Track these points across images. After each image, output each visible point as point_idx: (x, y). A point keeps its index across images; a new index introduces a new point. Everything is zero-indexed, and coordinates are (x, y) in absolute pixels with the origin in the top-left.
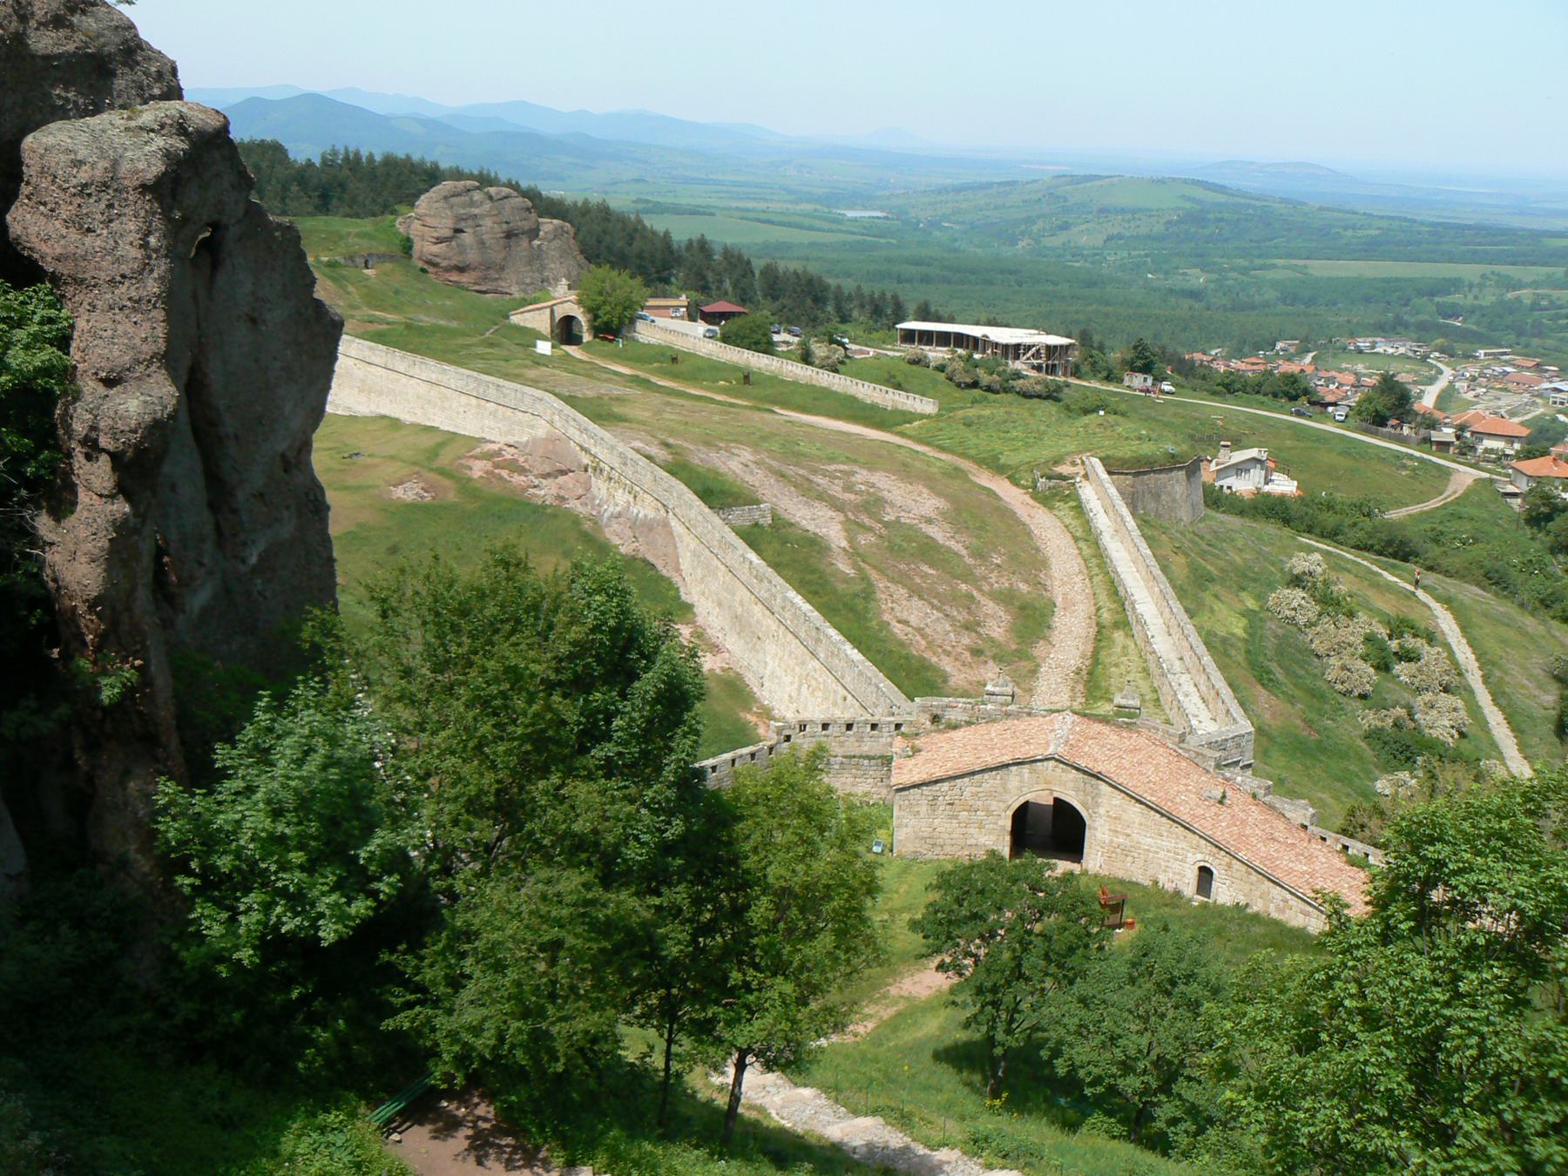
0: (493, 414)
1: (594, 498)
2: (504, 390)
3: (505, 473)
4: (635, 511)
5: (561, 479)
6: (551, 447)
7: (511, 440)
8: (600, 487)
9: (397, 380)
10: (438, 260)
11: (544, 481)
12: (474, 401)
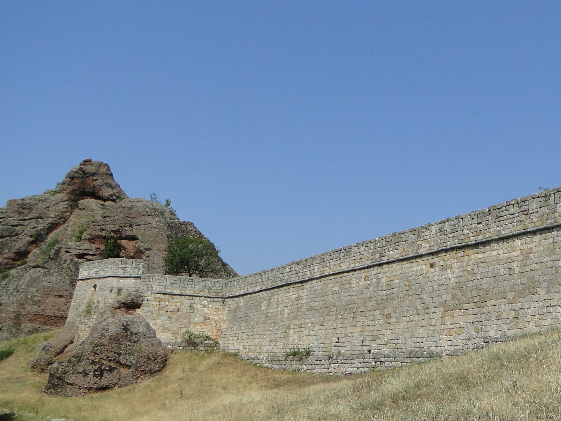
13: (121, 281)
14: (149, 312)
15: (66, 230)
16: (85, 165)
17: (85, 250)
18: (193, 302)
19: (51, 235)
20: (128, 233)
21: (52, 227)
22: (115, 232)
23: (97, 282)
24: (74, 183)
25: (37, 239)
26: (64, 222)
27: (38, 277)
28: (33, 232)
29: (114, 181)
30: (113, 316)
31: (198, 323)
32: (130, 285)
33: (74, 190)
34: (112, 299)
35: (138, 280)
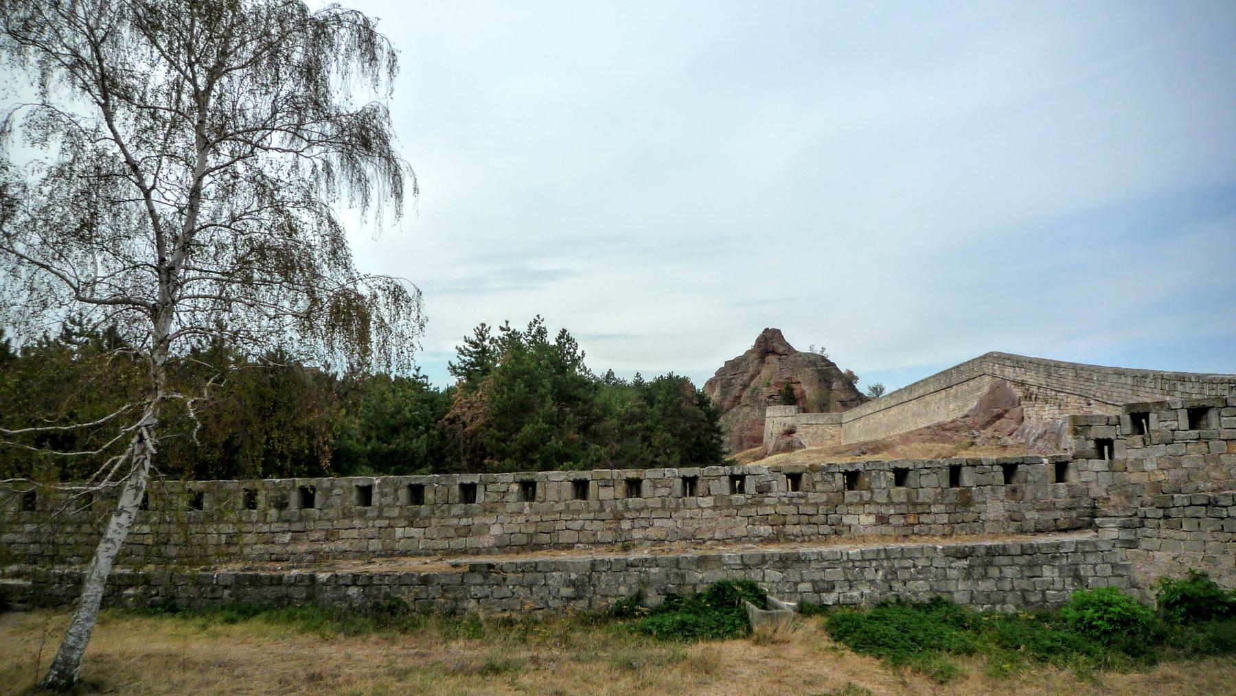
0: (956, 397)
1: (1024, 430)
3: (949, 434)
5: (997, 422)
6: (991, 397)
7: (965, 411)
8: (1030, 411)
11: (982, 431)
12: (944, 393)
19: (752, 383)
21: (753, 377)
25: (745, 386)
28: (741, 382)
32: (790, 421)
33: (762, 351)
34: (781, 429)
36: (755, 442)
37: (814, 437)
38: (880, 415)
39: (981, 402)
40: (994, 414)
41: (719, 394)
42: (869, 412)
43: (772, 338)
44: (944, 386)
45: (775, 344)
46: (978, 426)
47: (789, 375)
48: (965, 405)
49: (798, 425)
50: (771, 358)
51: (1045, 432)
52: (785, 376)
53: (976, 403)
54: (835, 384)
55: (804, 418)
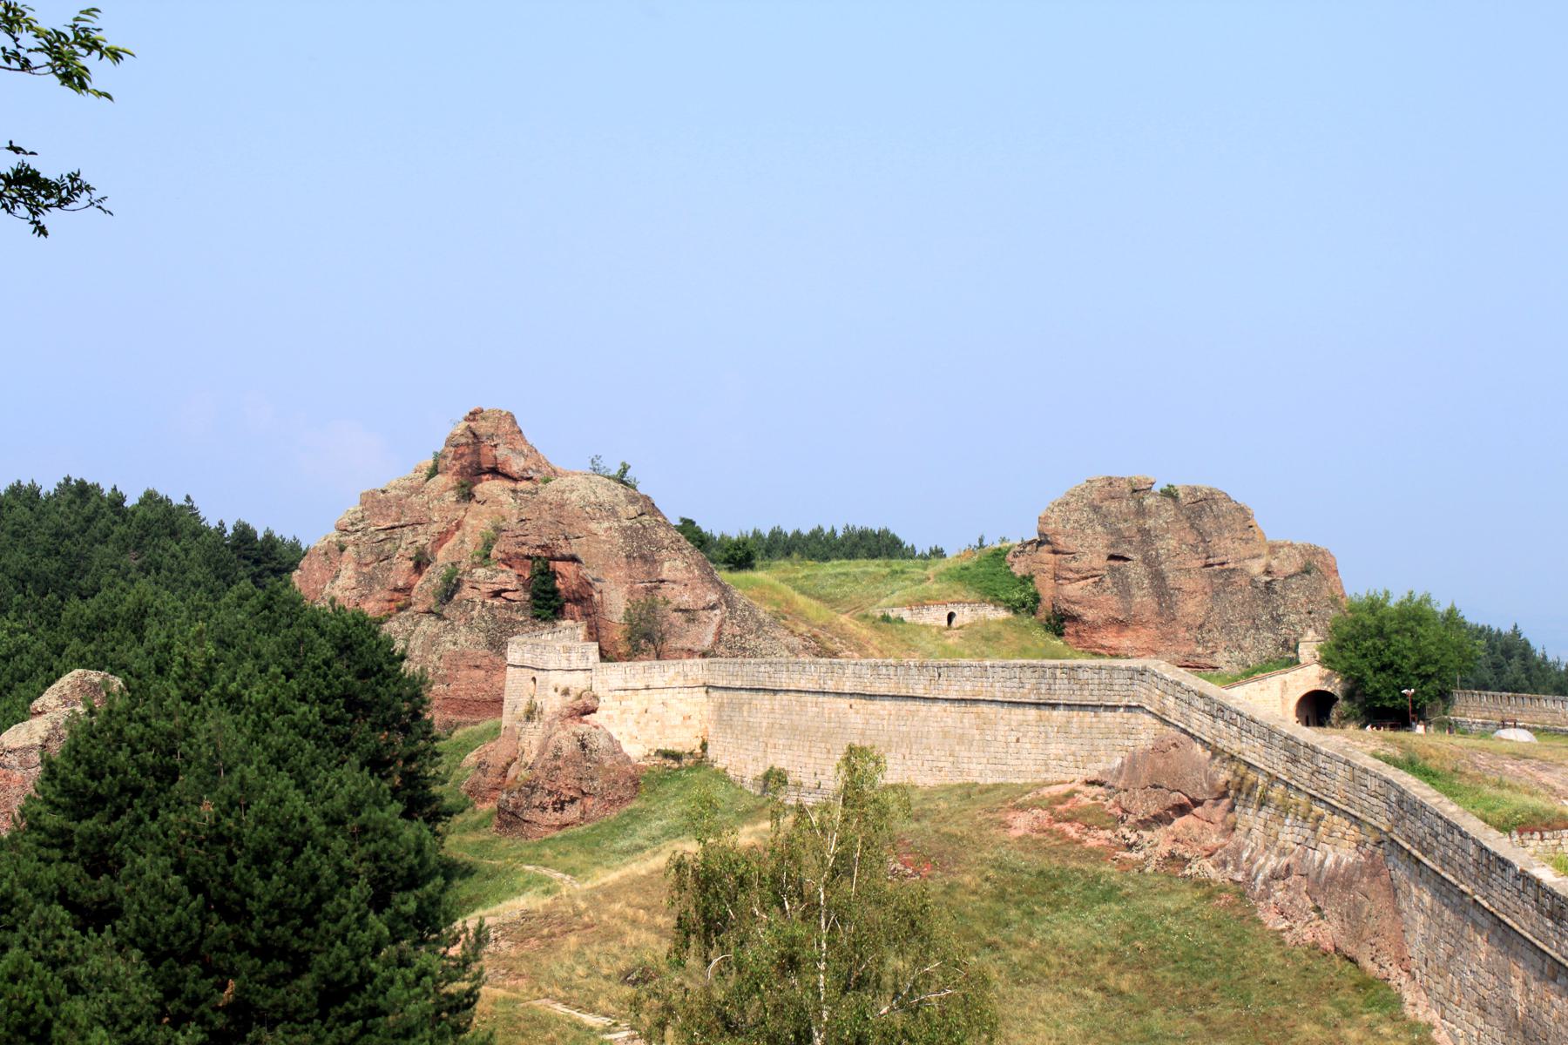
0: (1064, 730)
2: (1082, 675)
3: (1071, 830)
4: (1318, 856)
5: (1179, 822)
9: (913, 714)
10: (1077, 610)
11: (1147, 835)
12: (1032, 713)
13: (568, 675)
14: (609, 717)
15: (463, 542)
16: (474, 420)
17: (501, 583)
18: (664, 697)
19: (441, 554)
20: (566, 552)
22: (543, 547)
23: (535, 674)
24: (462, 455)
26: (458, 526)
27: (437, 636)
29: (525, 443)
30: (565, 728)
31: (674, 727)
33: (463, 467)
35: (588, 673)
36: (461, 713)
37: (643, 720)
38: (843, 703)
39: (1132, 764)
40: (1169, 804)
41: (353, 583)
42: (803, 685)
43: (491, 437)
44: (1033, 699)
45: (502, 452)
46: (1131, 819)
47: (545, 540)
48: (1092, 756)
49: (598, 689)
50: (489, 487)
51: (1288, 868)
52: (534, 539)
53: (1119, 761)
54: (667, 565)
55: (617, 674)
